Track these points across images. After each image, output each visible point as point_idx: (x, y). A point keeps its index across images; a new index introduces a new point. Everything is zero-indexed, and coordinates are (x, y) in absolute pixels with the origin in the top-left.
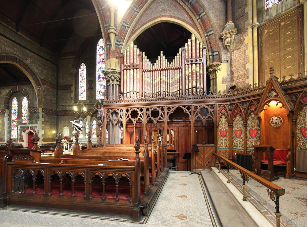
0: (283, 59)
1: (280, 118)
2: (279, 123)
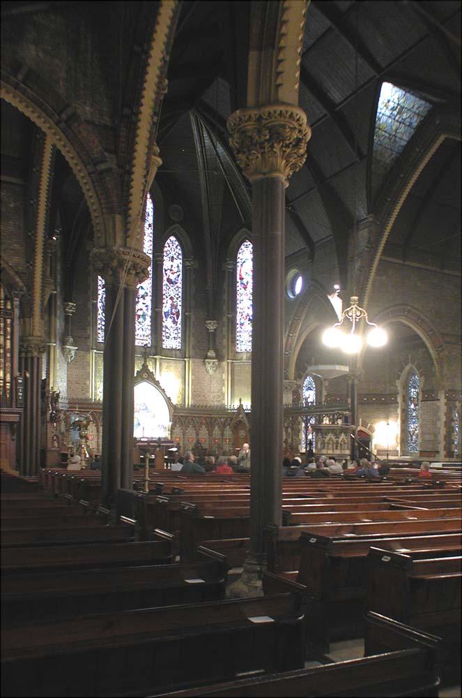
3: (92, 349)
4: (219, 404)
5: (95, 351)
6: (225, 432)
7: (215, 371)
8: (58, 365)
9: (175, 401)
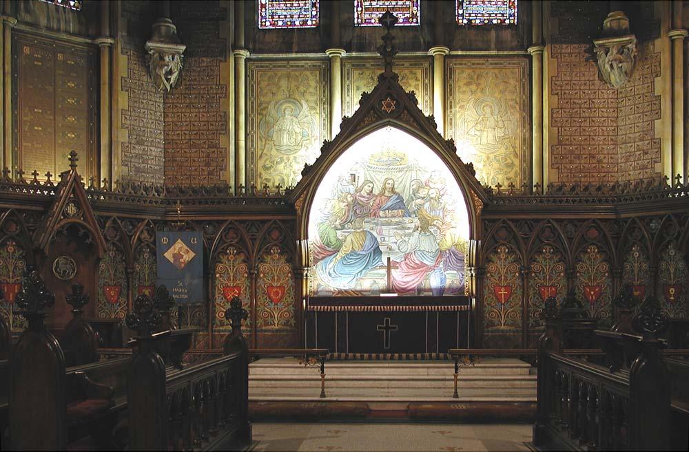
0: (61, 134)
1: (72, 262)
2: (69, 272)
3: (236, 47)
4: (645, 176)
5: (245, 54)
6: (663, 265)
7: (628, 74)
8: (123, 100)
9: (486, 175)
